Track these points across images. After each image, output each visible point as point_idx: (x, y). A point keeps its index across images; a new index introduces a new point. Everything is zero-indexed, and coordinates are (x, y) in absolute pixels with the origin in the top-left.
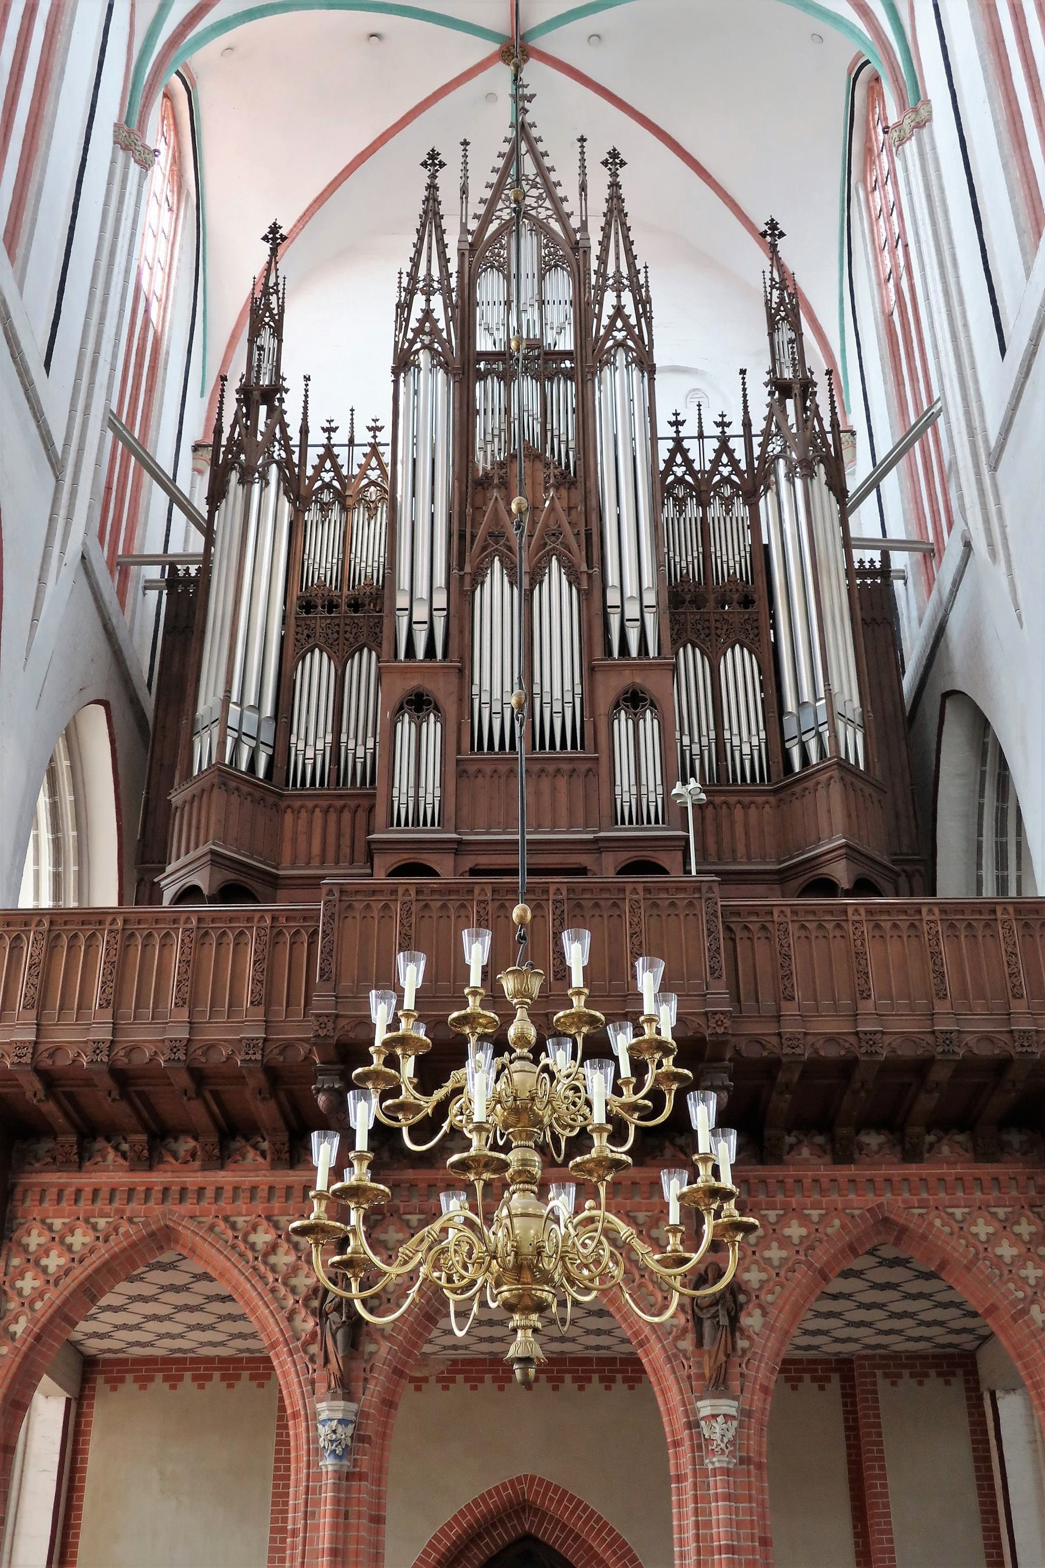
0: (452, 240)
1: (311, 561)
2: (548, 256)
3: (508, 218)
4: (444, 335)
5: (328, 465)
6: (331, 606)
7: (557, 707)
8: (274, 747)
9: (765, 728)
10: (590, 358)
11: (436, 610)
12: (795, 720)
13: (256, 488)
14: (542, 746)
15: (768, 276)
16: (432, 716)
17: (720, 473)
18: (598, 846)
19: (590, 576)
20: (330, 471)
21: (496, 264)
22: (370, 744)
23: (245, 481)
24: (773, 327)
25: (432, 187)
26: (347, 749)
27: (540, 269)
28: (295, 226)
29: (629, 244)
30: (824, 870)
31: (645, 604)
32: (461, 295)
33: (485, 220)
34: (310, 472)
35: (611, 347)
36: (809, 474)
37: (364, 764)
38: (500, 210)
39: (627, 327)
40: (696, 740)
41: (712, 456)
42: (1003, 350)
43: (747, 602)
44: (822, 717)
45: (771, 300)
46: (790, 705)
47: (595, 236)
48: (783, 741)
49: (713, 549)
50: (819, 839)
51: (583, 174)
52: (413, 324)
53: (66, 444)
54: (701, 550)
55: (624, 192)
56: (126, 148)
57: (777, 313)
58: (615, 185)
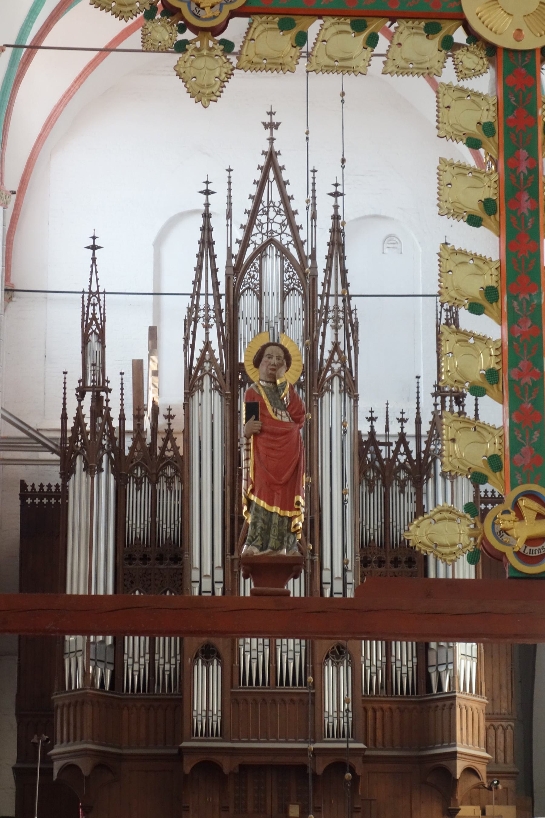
0: (221, 262)
1: (130, 523)
3: (259, 242)
6: (145, 558)
7: (291, 655)
8: (114, 664)
11: (216, 582)
12: (434, 653)
14: (281, 684)
16: (215, 661)
17: (399, 460)
19: (312, 561)
21: (252, 286)
22: (173, 661)
25: (207, 216)
26: (159, 665)
28: (72, 86)
29: (344, 272)
30: (444, 763)
32: (229, 331)
33: (244, 244)
37: (170, 676)
38: (254, 235)
45: (440, 319)
47: (321, 263)
48: (427, 666)
49: (391, 520)
50: (443, 742)
52: (197, 354)
54: (383, 520)
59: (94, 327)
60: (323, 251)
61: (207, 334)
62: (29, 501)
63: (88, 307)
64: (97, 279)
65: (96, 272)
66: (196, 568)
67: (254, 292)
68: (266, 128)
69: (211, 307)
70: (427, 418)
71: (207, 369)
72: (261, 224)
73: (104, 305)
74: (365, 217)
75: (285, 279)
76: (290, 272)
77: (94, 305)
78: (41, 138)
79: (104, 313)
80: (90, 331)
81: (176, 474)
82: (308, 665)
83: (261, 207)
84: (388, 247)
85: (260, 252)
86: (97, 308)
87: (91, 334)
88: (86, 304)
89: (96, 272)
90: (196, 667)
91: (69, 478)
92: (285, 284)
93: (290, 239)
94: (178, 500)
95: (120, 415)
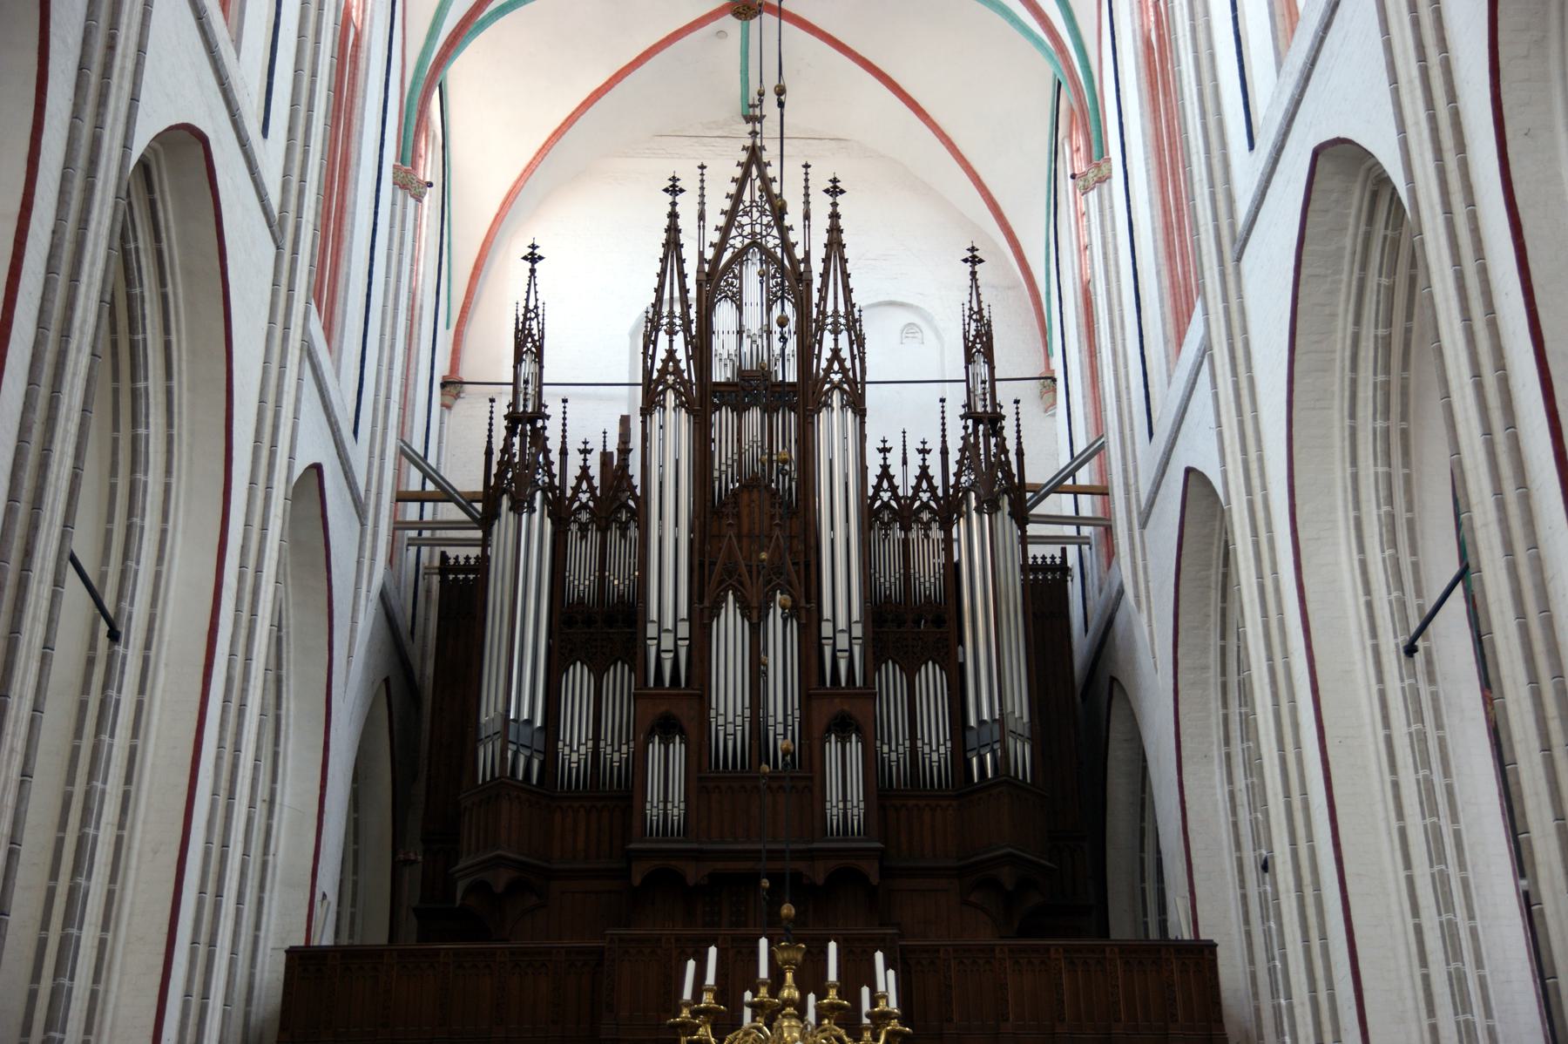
0: (691, 268)
2: (775, 287)
3: (739, 245)
4: (686, 375)
5: (584, 486)
8: (545, 753)
9: (951, 739)
10: (810, 402)
13: (524, 516)
15: (967, 306)
18: (810, 855)
19: (808, 610)
20: (586, 492)
21: (730, 294)
22: (624, 749)
23: (516, 508)
24: (969, 359)
25: (673, 216)
27: (768, 300)
28: (534, 158)
29: (846, 276)
31: (853, 635)
33: (720, 248)
34: (569, 493)
35: (829, 390)
36: (994, 508)
38: (732, 238)
39: (843, 370)
40: (893, 748)
41: (912, 482)
42: (1151, 434)
43: (939, 621)
44: (997, 736)
45: (969, 331)
46: (973, 722)
47: (817, 267)
48: (965, 751)
49: (912, 571)
51: (807, 203)
52: (658, 365)
53: (367, 490)
55: (842, 223)
56: (404, 187)
57: (973, 346)
58: (835, 216)
59: (529, 345)
60: (818, 254)
61: (671, 341)
62: (451, 577)
63: (524, 323)
64: (536, 292)
65: (535, 285)
66: (653, 621)
67: (732, 301)
68: (747, 122)
69: (677, 314)
70: (954, 445)
71: (670, 382)
72: (741, 226)
73: (543, 319)
74: (880, 304)
75: (771, 286)
76: (778, 278)
77: (531, 319)
78: (499, 219)
79: (543, 328)
80: (525, 349)
81: (632, 518)
82: (803, 742)
83: (741, 207)
84: (907, 337)
85: (740, 257)
86: (534, 324)
87: (526, 352)
88: (521, 319)
89: (535, 285)
90: (651, 745)
91: (492, 525)
92: (772, 292)
93: (778, 241)
94: (635, 558)
95: (561, 449)
